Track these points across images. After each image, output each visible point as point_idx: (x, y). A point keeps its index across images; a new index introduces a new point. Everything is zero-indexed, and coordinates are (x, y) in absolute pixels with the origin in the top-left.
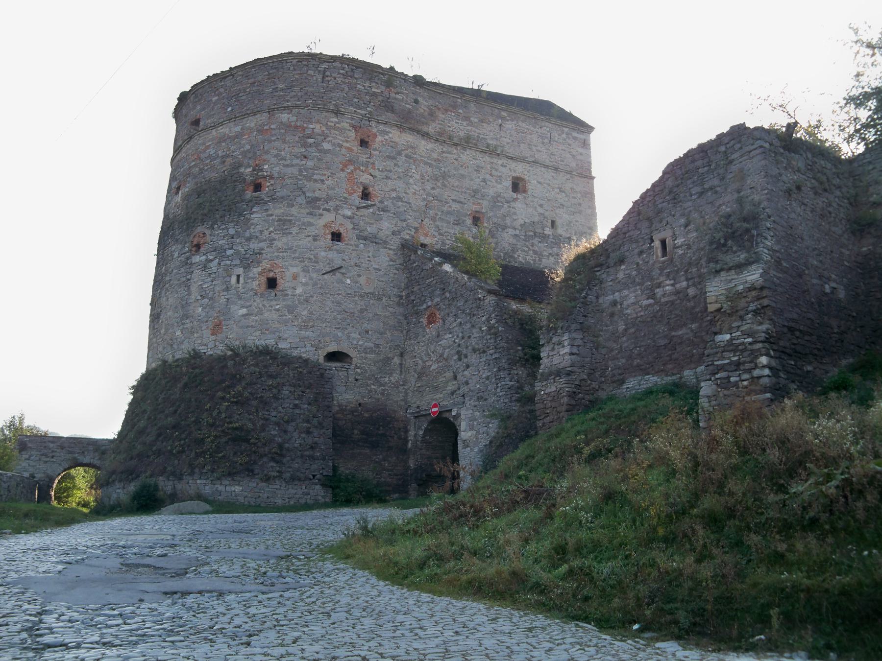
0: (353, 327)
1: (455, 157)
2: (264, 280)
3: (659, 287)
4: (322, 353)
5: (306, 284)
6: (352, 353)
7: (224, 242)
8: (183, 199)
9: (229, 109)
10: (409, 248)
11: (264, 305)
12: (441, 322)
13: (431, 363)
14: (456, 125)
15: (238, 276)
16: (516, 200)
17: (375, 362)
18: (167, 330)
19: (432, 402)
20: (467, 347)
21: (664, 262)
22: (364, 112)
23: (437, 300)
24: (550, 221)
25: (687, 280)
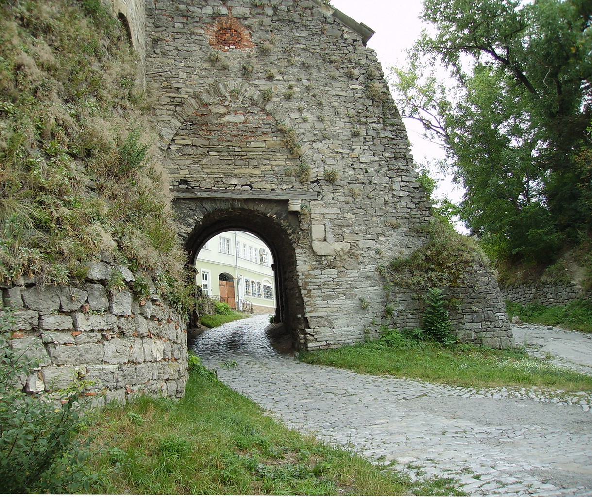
13: (222, 110)
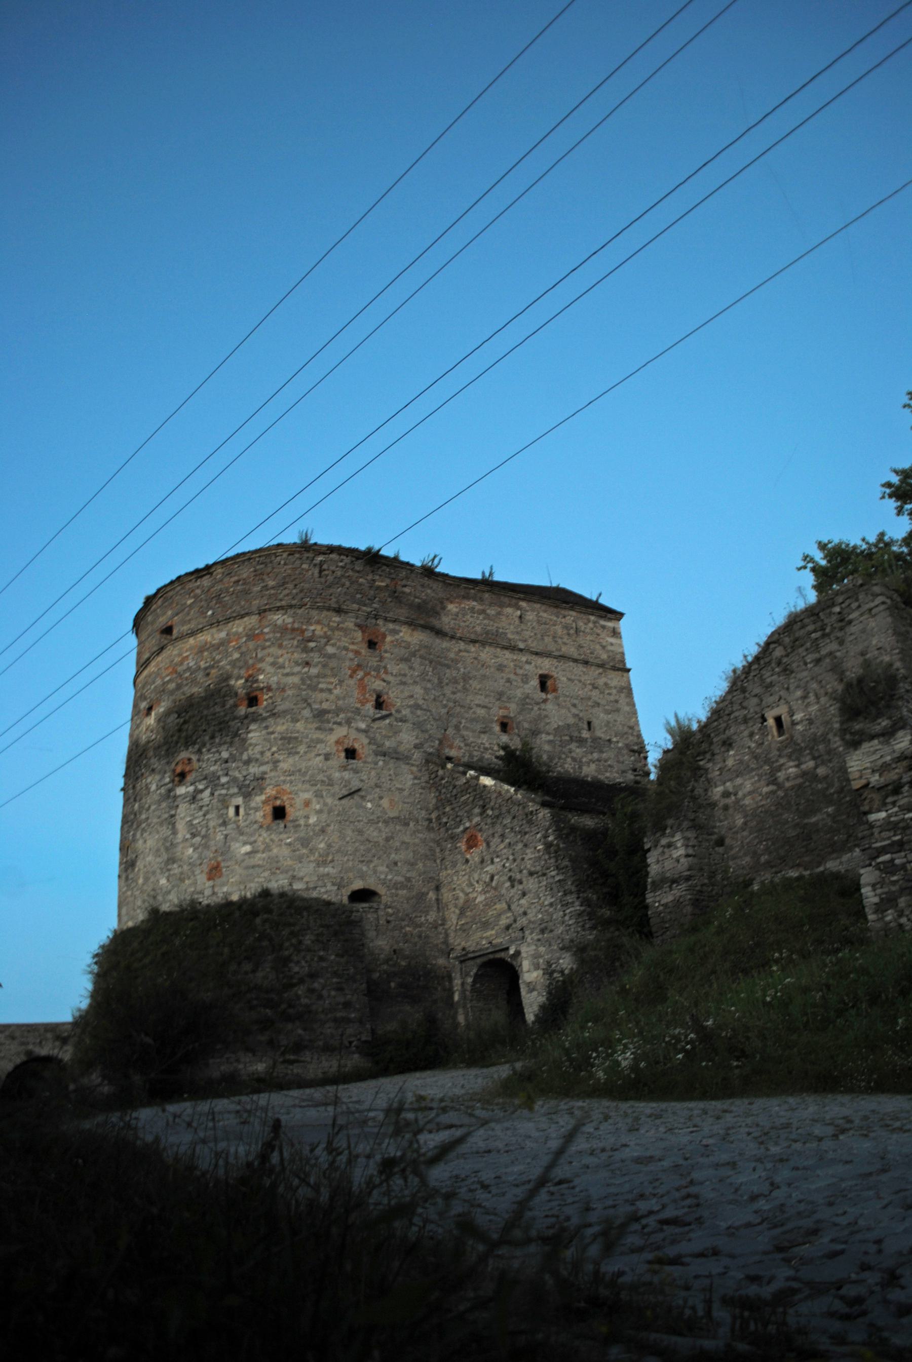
0: (379, 858)
1: (474, 655)
2: (269, 809)
3: (780, 771)
4: (346, 893)
5: (319, 812)
6: (381, 890)
7: (216, 767)
8: (159, 720)
9: (210, 613)
10: (437, 760)
11: (272, 840)
12: (484, 845)
13: (475, 895)
14: (471, 619)
15: (237, 808)
16: (545, 701)
17: (408, 899)
18: (146, 879)
19: (481, 940)
20: (521, 872)
21: (781, 742)
22: (369, 610)
23: (476, 819)
24: (586, 723)
25: (814, 758)
